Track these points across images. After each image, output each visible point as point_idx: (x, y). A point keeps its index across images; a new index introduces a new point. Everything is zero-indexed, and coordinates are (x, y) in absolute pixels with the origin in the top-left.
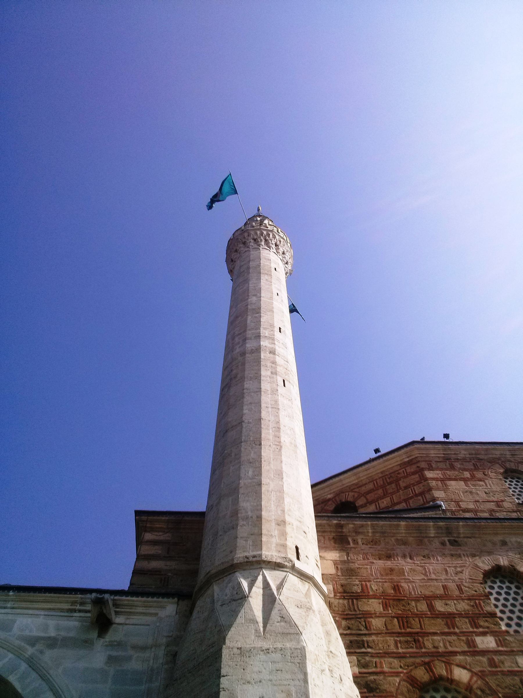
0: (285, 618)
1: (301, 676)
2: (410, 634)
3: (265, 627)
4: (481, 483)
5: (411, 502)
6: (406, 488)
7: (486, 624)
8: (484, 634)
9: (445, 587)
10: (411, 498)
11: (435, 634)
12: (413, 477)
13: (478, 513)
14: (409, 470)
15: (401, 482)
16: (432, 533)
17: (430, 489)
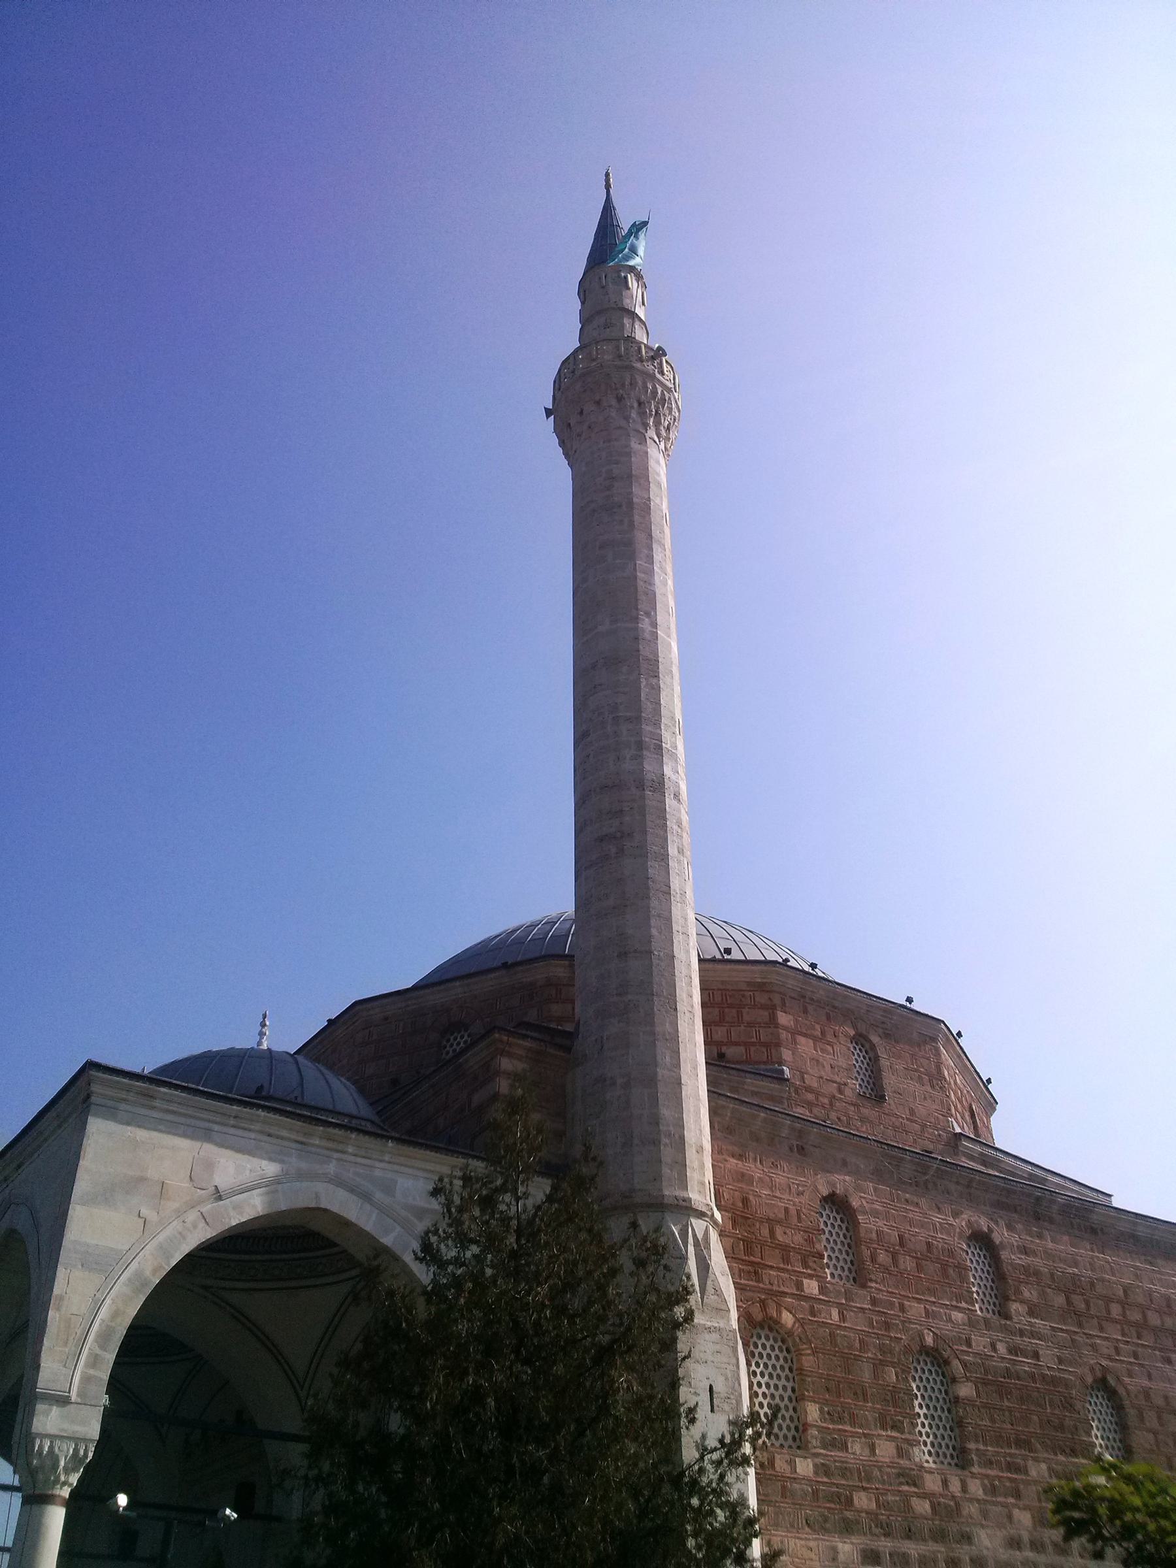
0: (718, 1292)
1: (734, 1361)
2: (752, 1263)
3: (702, 1299)
4: (829, 1048)
5: (753, 1049)
6: (750, 1025)
7: (815, 1266)
8: (810, 1277)
9: (786, 1209)
10: (753, 1044)
11: (772, 1267)
12: (761, 1012)
13: (821, 1098)
14: (762, 998)
15: (745, 1011)
16: (785, 1133)
17: (778, 1045)
